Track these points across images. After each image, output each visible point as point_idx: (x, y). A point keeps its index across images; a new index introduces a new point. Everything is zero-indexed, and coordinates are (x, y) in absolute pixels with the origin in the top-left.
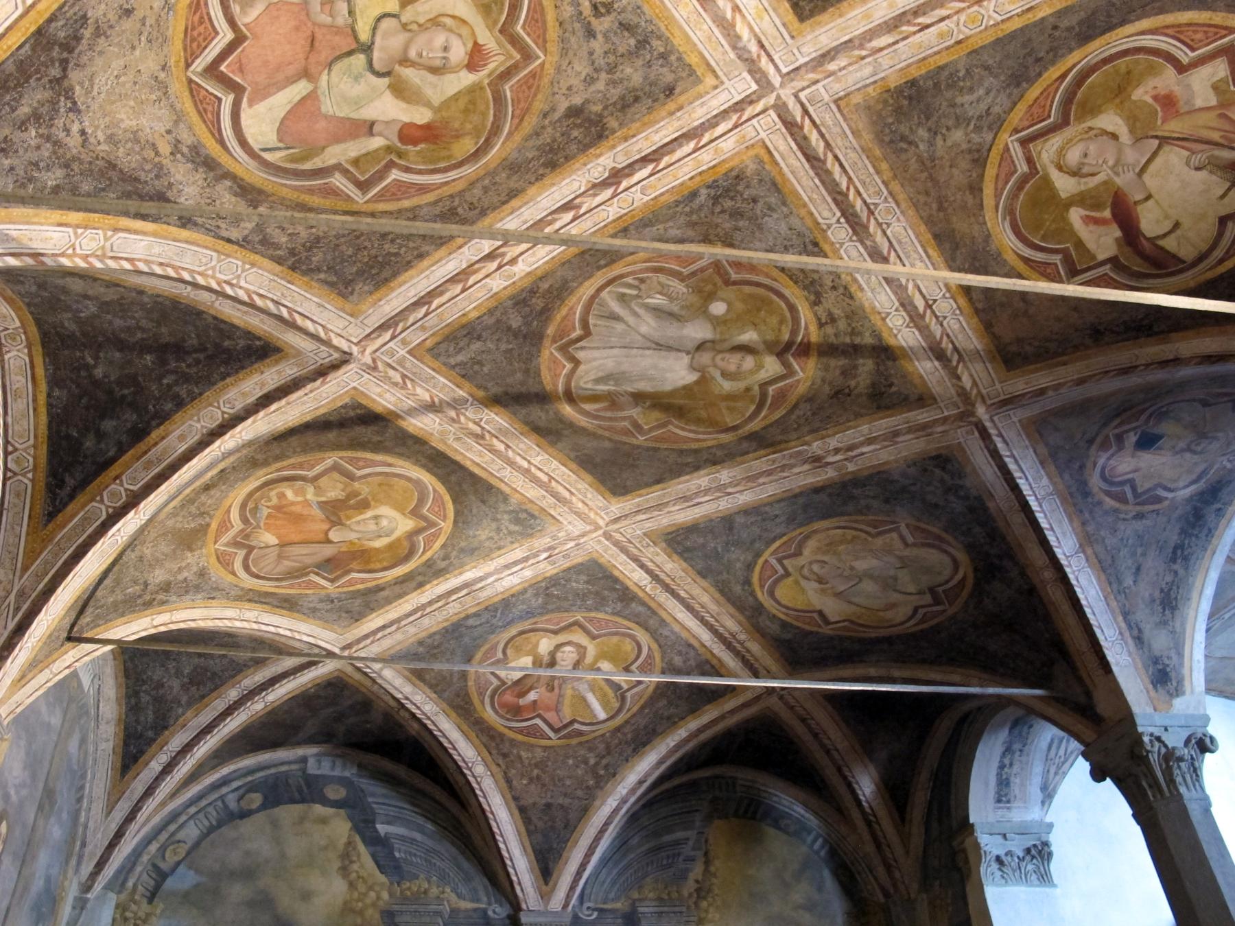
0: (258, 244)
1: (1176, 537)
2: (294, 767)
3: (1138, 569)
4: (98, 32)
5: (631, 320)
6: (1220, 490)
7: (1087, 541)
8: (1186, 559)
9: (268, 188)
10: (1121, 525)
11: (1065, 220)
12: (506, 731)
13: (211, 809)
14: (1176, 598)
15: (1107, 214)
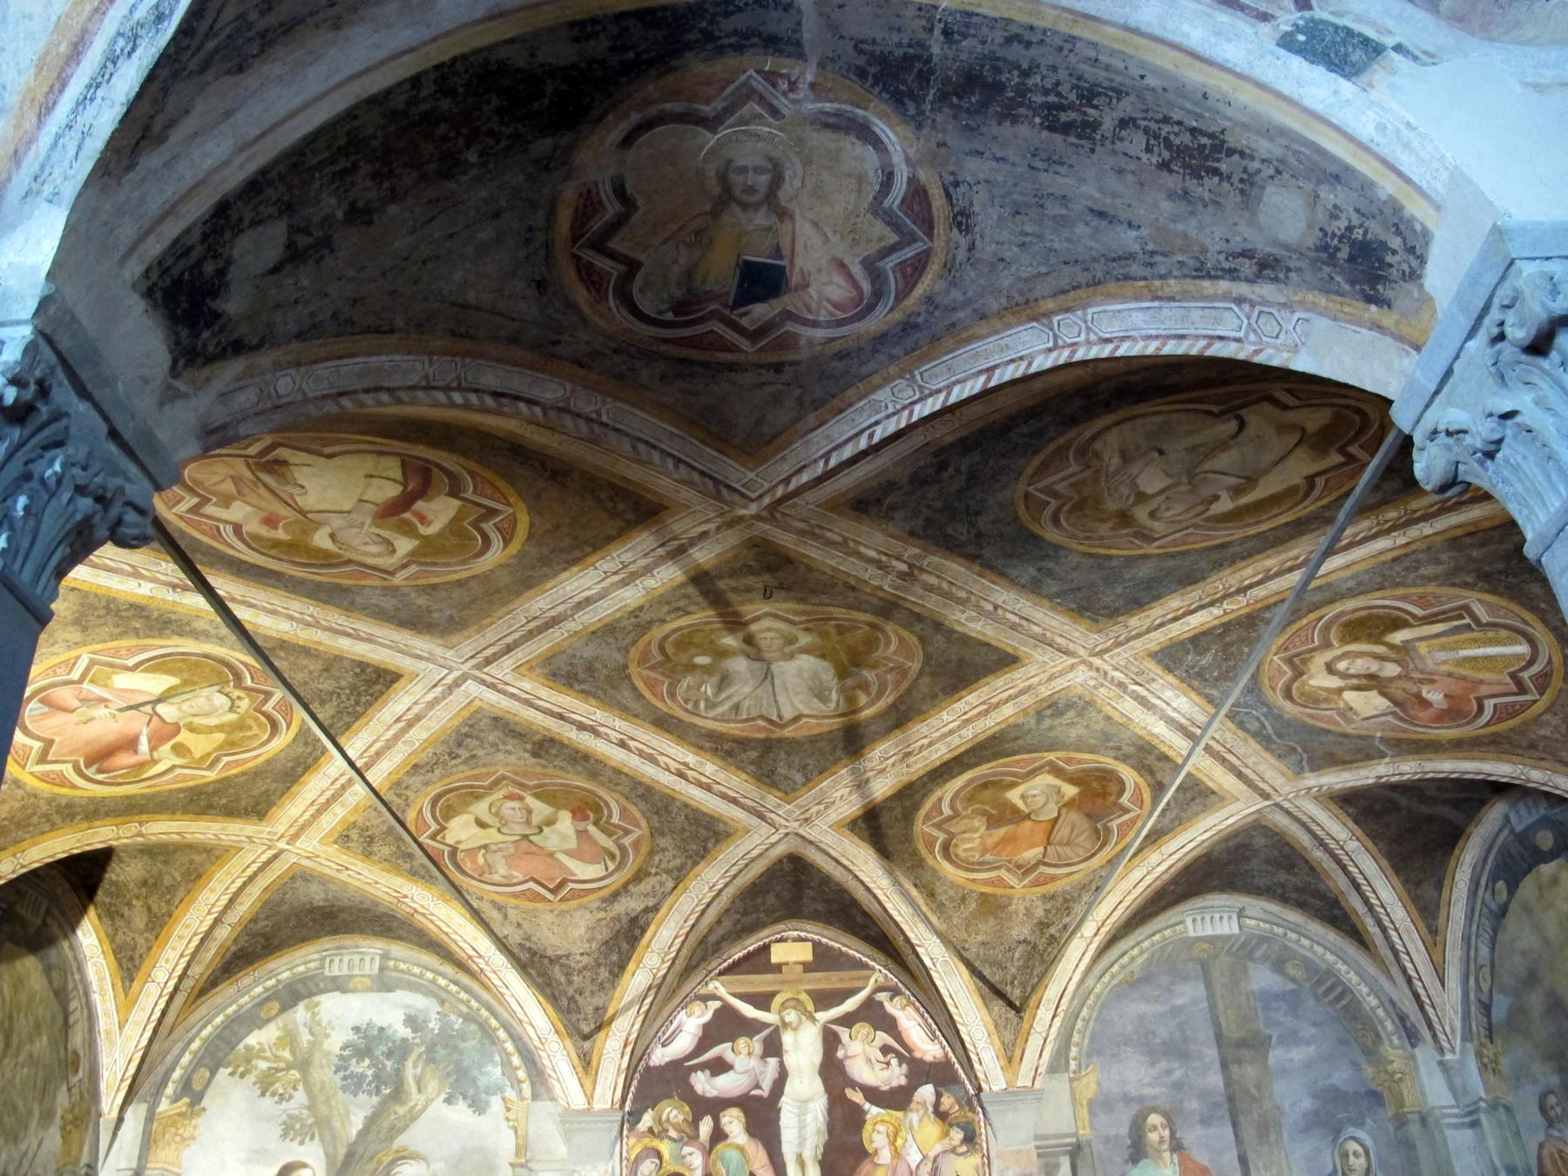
0: (680, 876)
1: (1024, 130)
2: (1506, 832)
3: (1101, 215)
4: (528, 939)
5: (736, 700)
6: (883, 60)
7: (1025, 307)
8: (1089, 95)
9: (636, 867)
10: (987, 249)
11: (440, 535)
12: (1493, 729)
13: (1484, 920)
14: (1194, 131)
15: (407, 515)
